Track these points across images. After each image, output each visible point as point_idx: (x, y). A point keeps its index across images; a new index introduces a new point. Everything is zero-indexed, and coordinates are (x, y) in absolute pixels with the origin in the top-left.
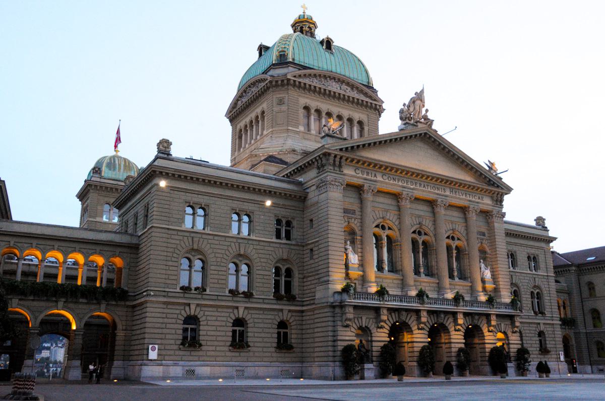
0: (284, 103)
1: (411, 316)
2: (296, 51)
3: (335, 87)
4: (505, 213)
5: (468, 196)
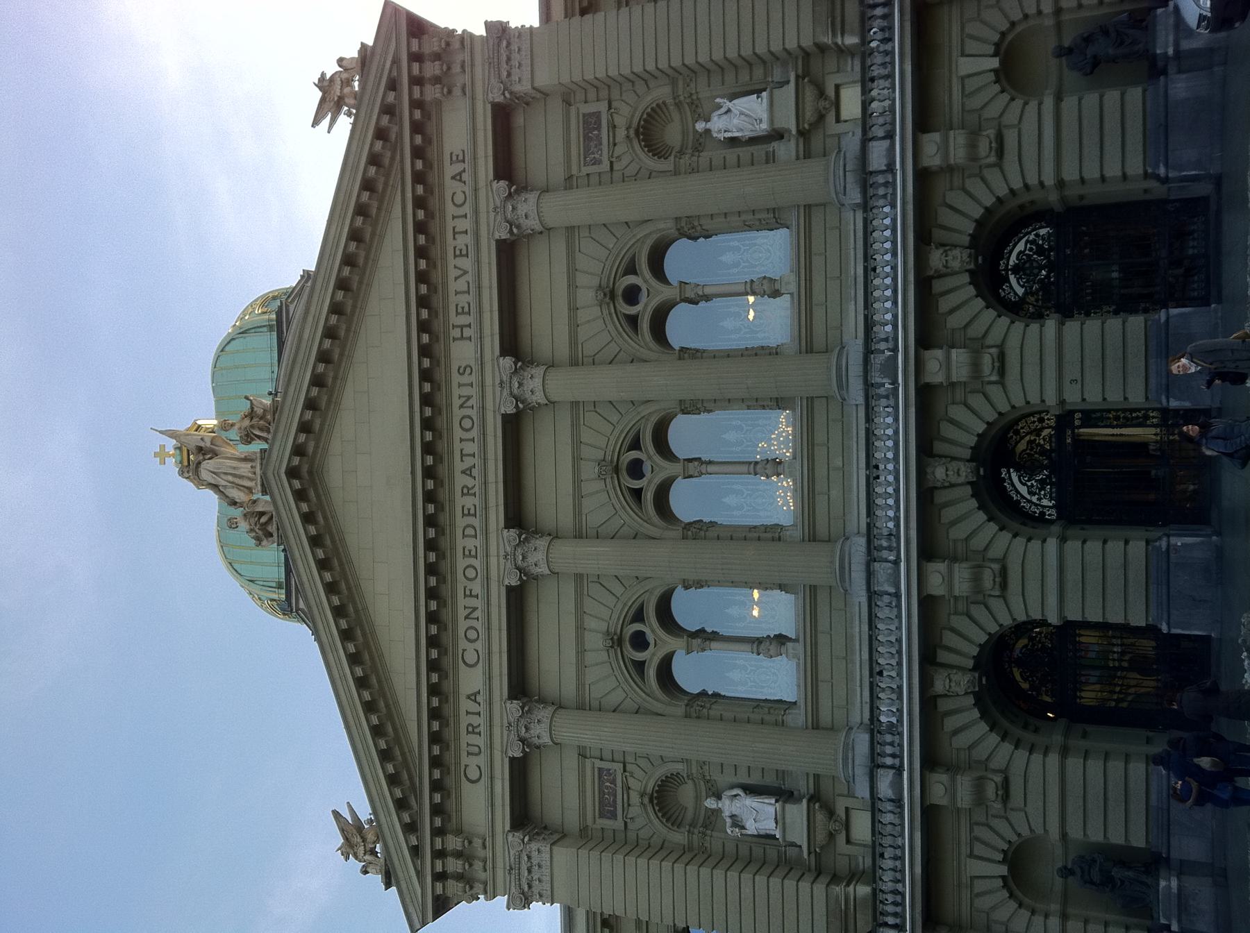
1: (953, 630)
4: (488, 25)
5: (462, 241)
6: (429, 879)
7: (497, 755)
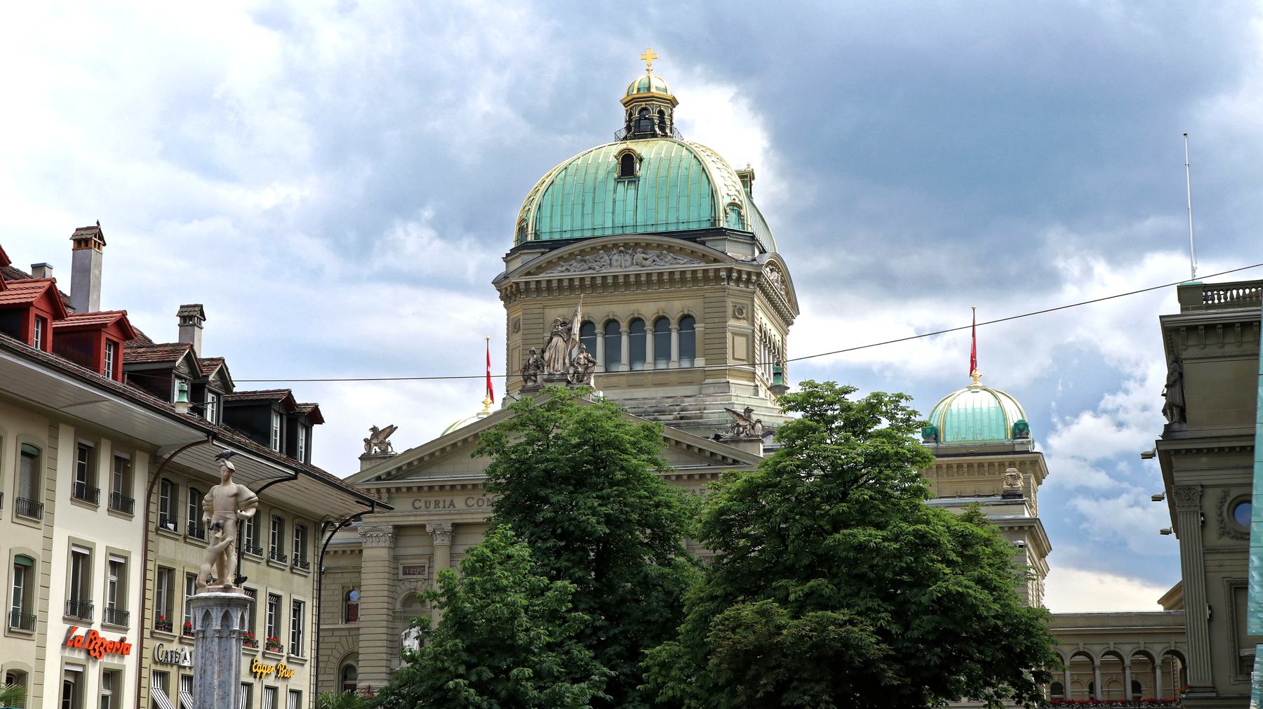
0: (519, 330)
2: (546, 211)
3: (620, 263)
6: (367, 487)
7: (426, 518)
